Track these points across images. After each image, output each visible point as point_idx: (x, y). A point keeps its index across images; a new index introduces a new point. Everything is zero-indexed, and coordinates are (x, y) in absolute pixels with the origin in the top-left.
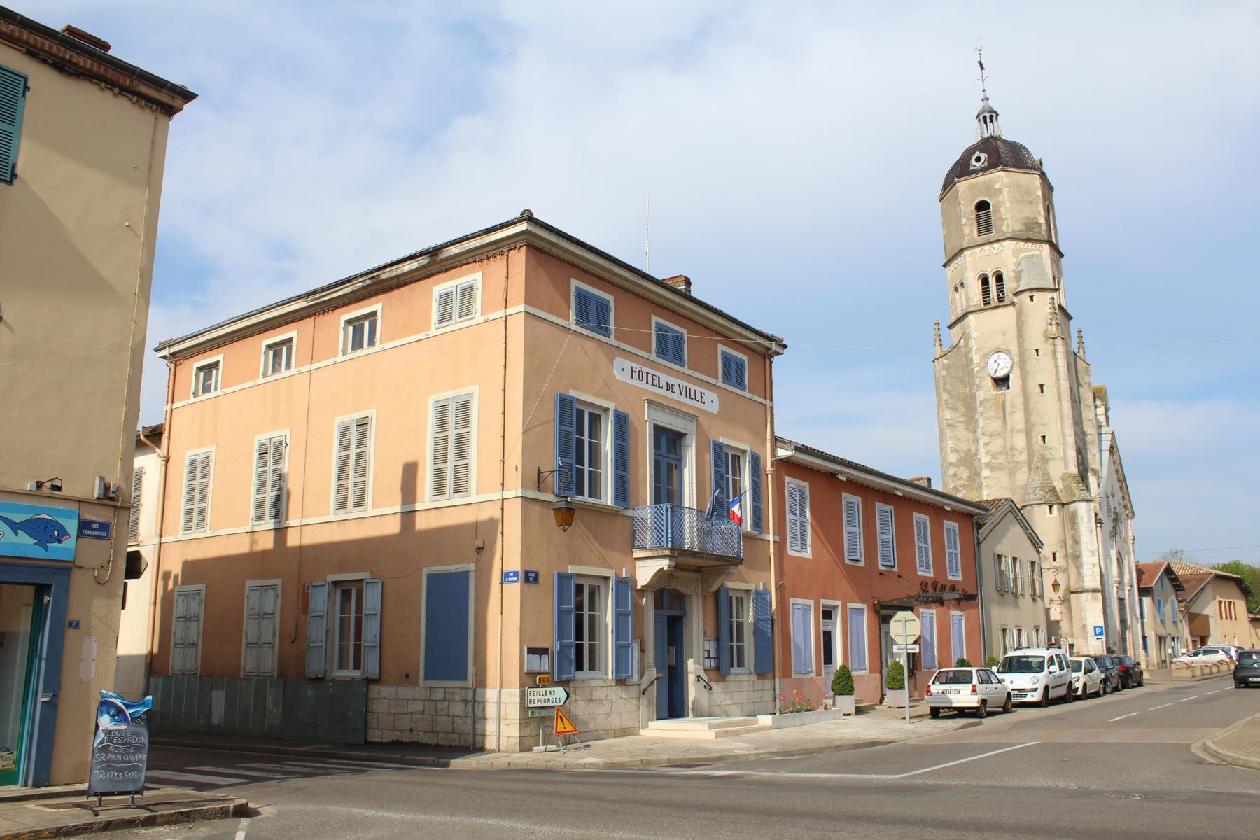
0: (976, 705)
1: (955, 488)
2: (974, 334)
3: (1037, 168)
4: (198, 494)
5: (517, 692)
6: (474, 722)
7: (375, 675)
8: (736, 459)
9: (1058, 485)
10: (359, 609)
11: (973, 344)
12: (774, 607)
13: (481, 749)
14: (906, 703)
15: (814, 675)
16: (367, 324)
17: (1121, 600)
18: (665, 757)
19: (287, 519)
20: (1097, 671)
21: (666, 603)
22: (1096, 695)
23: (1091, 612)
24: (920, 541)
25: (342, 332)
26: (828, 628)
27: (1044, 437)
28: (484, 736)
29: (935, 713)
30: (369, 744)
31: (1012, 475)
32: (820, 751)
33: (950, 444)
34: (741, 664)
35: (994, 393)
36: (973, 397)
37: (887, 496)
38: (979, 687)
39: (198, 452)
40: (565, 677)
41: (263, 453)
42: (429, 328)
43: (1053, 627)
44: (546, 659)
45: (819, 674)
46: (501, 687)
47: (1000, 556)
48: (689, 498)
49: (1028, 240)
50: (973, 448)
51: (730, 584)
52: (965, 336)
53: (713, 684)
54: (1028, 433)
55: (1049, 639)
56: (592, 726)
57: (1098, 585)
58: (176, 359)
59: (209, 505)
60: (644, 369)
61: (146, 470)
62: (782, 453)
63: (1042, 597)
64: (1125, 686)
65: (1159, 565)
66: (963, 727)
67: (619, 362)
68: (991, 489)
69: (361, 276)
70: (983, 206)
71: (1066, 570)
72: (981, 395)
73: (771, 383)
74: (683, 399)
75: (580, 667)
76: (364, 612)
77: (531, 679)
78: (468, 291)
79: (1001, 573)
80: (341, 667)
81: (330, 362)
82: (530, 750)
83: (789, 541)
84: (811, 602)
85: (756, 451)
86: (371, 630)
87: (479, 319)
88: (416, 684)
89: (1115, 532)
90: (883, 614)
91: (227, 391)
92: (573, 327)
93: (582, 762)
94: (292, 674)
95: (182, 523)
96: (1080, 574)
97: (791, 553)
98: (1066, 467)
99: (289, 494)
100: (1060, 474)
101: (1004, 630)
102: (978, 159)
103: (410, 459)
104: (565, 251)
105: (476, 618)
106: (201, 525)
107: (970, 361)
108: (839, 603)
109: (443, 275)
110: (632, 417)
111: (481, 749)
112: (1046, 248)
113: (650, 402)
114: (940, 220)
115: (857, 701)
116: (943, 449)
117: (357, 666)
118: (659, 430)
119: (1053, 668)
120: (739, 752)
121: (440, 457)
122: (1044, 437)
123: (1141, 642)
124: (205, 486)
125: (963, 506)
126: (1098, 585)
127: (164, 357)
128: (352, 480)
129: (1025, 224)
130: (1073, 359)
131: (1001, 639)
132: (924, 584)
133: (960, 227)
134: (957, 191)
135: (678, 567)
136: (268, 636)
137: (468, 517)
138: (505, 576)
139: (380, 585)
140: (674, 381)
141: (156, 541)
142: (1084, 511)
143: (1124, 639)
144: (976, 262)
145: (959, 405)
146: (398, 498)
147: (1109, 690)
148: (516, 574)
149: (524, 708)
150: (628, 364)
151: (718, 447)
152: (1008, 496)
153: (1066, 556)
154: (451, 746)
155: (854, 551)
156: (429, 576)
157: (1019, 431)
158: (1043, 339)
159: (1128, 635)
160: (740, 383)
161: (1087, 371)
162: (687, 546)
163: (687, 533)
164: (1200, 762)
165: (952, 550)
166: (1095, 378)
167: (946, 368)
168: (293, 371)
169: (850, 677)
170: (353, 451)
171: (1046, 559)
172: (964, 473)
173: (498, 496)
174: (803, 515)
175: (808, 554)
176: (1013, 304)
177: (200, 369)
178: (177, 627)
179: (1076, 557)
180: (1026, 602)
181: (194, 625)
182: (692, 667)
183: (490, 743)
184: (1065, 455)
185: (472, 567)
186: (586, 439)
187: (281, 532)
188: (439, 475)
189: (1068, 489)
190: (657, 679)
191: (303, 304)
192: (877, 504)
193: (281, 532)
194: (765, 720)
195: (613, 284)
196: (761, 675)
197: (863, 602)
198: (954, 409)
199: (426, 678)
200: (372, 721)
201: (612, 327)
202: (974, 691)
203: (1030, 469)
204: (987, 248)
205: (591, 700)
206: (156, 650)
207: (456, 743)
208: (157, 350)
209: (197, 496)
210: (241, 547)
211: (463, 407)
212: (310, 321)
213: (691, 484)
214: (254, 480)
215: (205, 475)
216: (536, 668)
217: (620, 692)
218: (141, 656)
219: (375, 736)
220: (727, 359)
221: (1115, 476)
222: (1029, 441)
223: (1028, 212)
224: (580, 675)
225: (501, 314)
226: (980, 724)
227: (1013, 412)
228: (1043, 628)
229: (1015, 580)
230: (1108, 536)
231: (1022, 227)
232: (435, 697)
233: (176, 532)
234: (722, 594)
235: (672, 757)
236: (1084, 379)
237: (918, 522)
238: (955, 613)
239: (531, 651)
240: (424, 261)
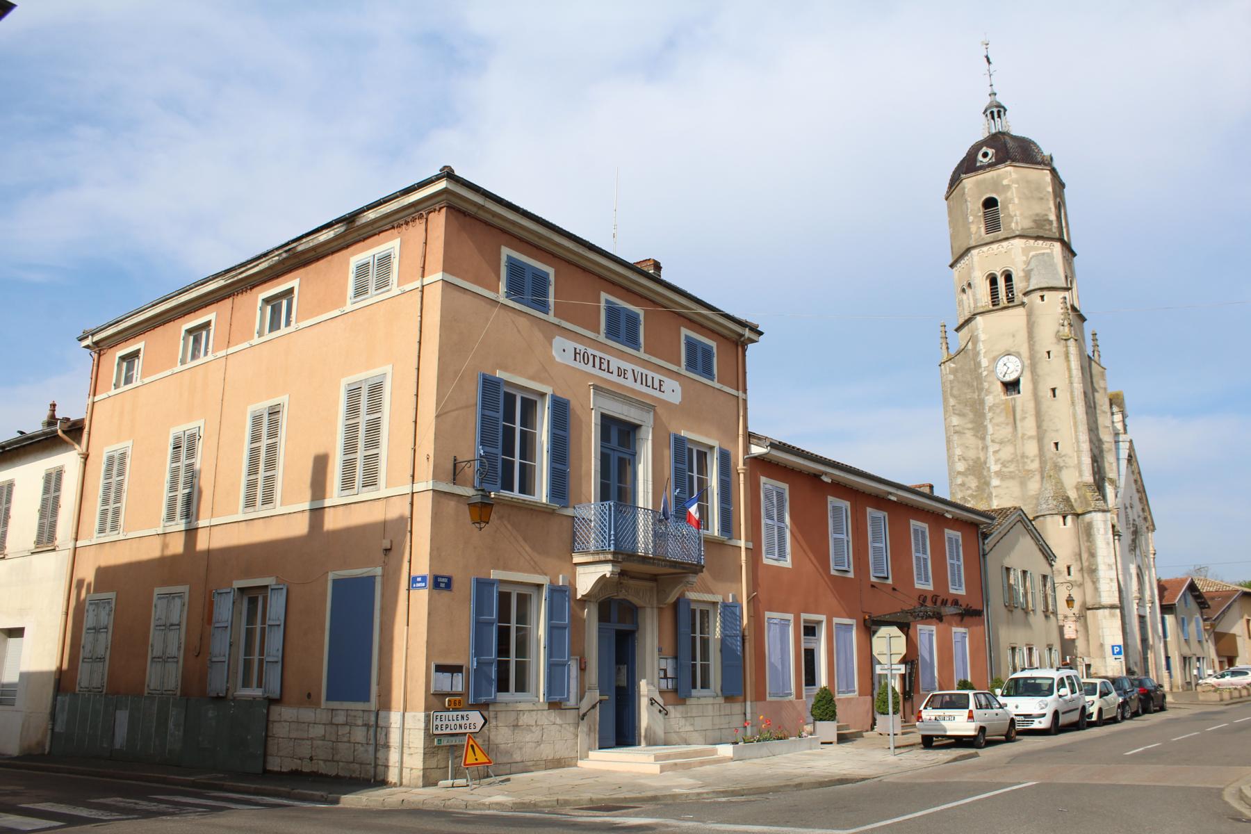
0: (973, 733)
1: (964, 498)
2: (982, 337)
3: (1047, 163)
4: (113, 493)
5: (422, 715)
6: (376, 751)
7: (276, 695)
8: (702, 456)
9: (1073, 495)
10: (263, 622)
11: (981, 347)
12: (745, 621)
13: (383, 783)
14: (899, 731)
15: (793, 697)
16: (285, 303)
17: (1142, 618)
18: (586, 796)
19: (197, 519)
20: (1114, 694)
21: (614, 615)
22: (1113, 720)
23: (1109, 630)
24: (917, 551)
25: (259, 312)
26: (810, 646)
27: (1056, 444)
28: (387, 767)
29: (928, 742)
30: (266, 774)
31: (1023, 484)
32: (776, 790)
33: (958, 452)
34: (705, 685)
35: (1004, 397)
36: (982, 402)
37: (880, 501)
38: (976, 713)
39: (114, 448)
40: (483, 699)
41: (177, 447)
42: (344, 303)
43: (1068, 646)
44: (459, 679)
45: (799, 696)
46: (405, 710)
47: (1008, 569)
48: (644, 495)
49: (1038, 238)
50: (982, 455)
51: (692, 595)
52: (973, 339)
53: (670, 708)
54: (1040, 439)
55: (1064, 659)
56: (517, 757)
57: (1116, 601)
58: (100, 348)
59: (123, 505)
60: (590, 351)
61: (66, 468)
62: (756, 450)
63: (1055, 613)
64: (1146, 711)
65: (1183, 581)
66: (955, 760)
67: (559, 342)
68: (1002, 497)
69: (277, 249)
70: (990, 203)
71: (1081, 585)
72: (989, 400)
73: (745, 373)
74: (638, 387)
75: (503, 686)
76: (268, 622)
77: (437, 701)
78: (385, 261)
79: (1010, 587)
80: (246, 684)
81: (246, 345)
82: (436, 784)
83: (764, 548)
84: (790, 617)
85: (726, 447)
86: (275, 641)
87: (395, 290)
88: (318, 704)
90: (870, 627)
91: (146, 380)
92: (502, 299)
93: (487, 800)
94: (195, 693)
95: (97, 526)
96: (1096, 589)
97: (767, 561)
98: (1081, 475)
99: (200, 492)
101: (1013, 649)
102: (985, 155)
103: (321, 451)
104: (495, 214)
105: (381, 630)
106: (114, 528)
107: (978, 365)
108: (823, 618)
109: (361, 244)
110: (574, 404)
111: (383, 783)
112: (1057, 245)
113: (596, 388)
114: (946, 218)
115: (839, 728)
116: (950, 456)
117: (260, 685)
118: (607, 422)
119: (1062, 691)
120: (677, 791)
121: (350, 447)
122: (1056, 444)
123: (1164, 662)
124: (120, 484)
125: (965, 514)
126: (1116, 601)
127: (87, 347)
128: (261, 474)
129: (1035, 221)
130: (1088, 363)
131: (1010, 658)
132: (923, 597)
133: (966, 224)
134: (964, 188)
135: (623, 573)
136: (173, 650)
137: (375, 515)
138: (412, 581)
139: (284, 591)
140: (625, 365)
141: (71, 545)
142: (1100, 523)
143: (1145, 659)
144: (984, 262)
145: (967, 410)
146: (308, 494)
147: (1128, 715)
148: (424, 579)
149: (429, 736)
150: (570, 345)
151: (680, 442)
152: (1017, 505)
154: (351, 778)
155: (841, 558)
156: (334, 581)
157: (1030, 438)
158: (1054, 340)
159: (1150, 655)
160: (708, 372)
161: (1103, 375)
162: (641, 552)
163: (641, 538)
164: (1238, 818)
165: (954, 562)
166: (1111, 383)
167: (954, 372)
168: (210, 357)
169: (831, 700)
170: (264, 442)
171: (1060, 572)
172: (973, 483)
173: (407, 489)
174: (781, 519)
175: (787, 563)
176: (1023, 304)
177: (123, 358)
178: (86, 639)
179: (1093, 571)
180: (1037, 619)
181: (102, 637)
182: (645, 688)
183: (393, 776)
184: (1080, 463)
185: (378, 571)
186: (518, 427)
187: (191, 533)
188: (349, 466)
189: (1083, 498)
190: (600, 701)
191: (220, 283)
192: (869, 510)
193: (191, 533)
194: (726, 750)
195: (554, 255)
196: (729, 698)
197: (850, 617)
199: (328, 699)
200: (272, 748)
201: (551, 300)
202: (971, 717)
203: (1042, 478)
204: (995, 246)
205: (516, 726)
206: (65, 666)
207: (356, 775)
208: (81, 340)
209: (112, 495)
210: (152, 551)
211: (376, 389)
212: (228, 302)
213: (646, 481)
214: (168, 477)
215: (121, 473)
216: (447, 688)
217: (554, 716)
218: (41, 674)
219: (274, 764)
220: (691, 344)
221: (1134, 486)
222: (1041, 448)
223: (1037, 208)
224: (502, 697)
225: (418, 284)
226: (976, 755)
227: (1024, 418)
228: (1057, 647)
229: (1025, 595)
230: (1127, 549)
232: (335, 721)
233: (91, 536)
234: (682, 608)
235: (594, 797)
236: (1099, 383)
237: (916, 531)
238: (958, 630)
239: (440, 668)
240: (339, 229)
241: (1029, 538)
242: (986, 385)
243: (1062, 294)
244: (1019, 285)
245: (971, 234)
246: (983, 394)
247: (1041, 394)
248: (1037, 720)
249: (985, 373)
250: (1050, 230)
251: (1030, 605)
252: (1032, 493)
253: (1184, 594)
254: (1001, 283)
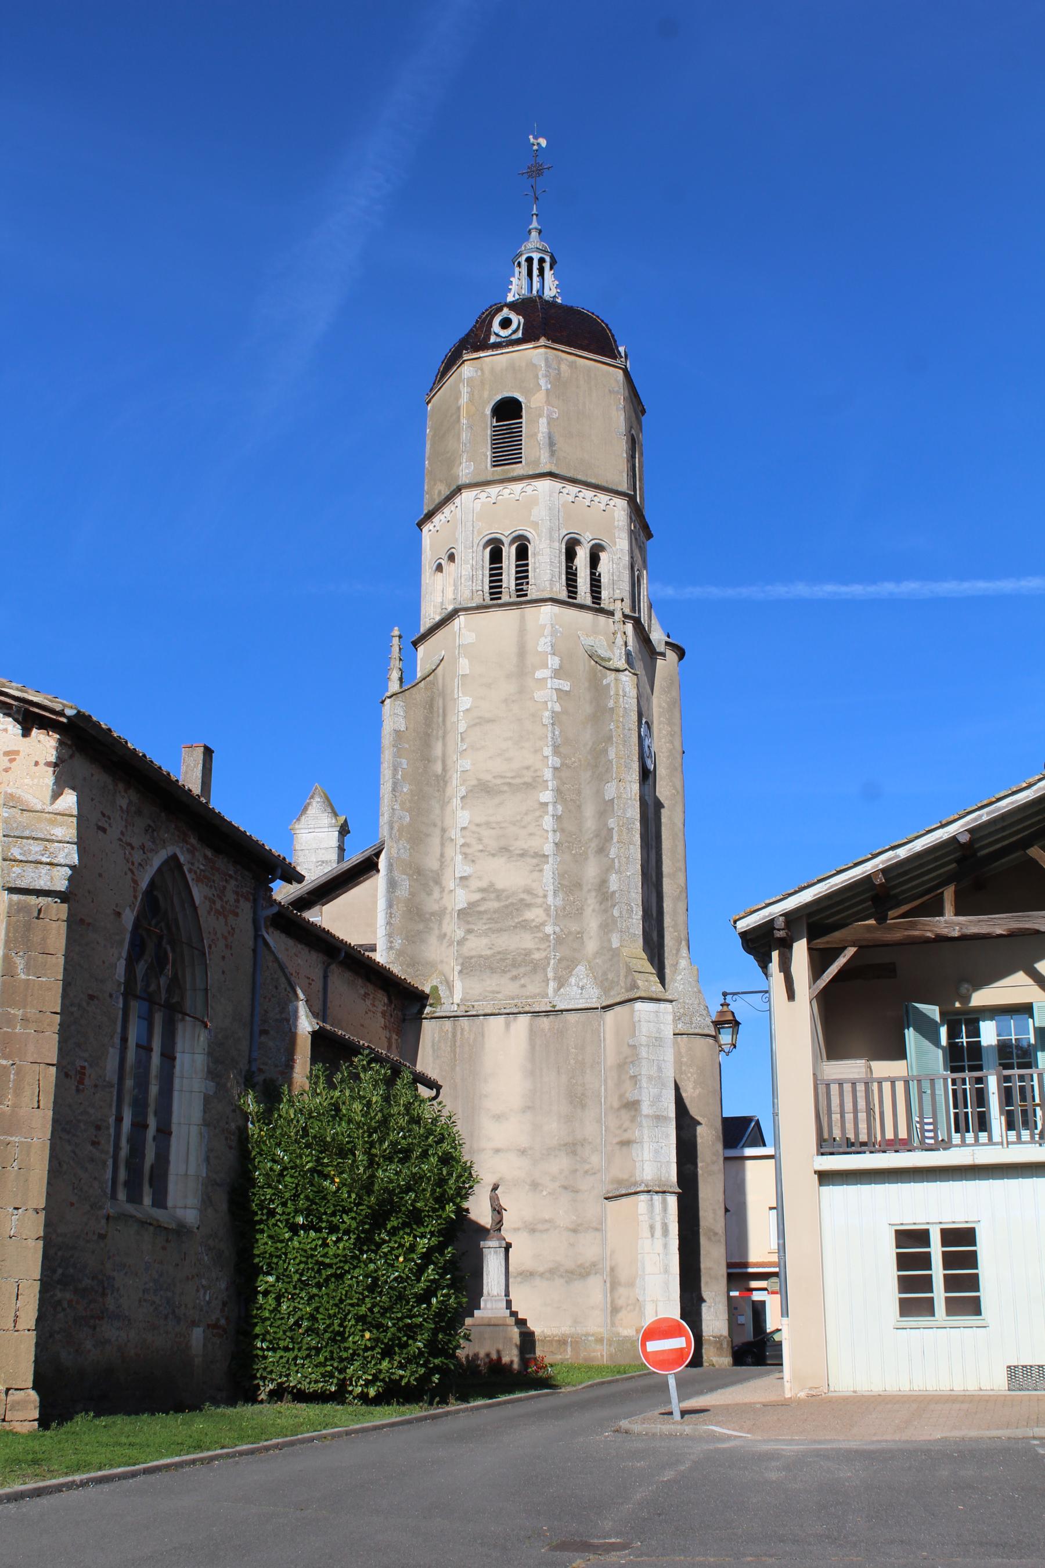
102: (506, 323)
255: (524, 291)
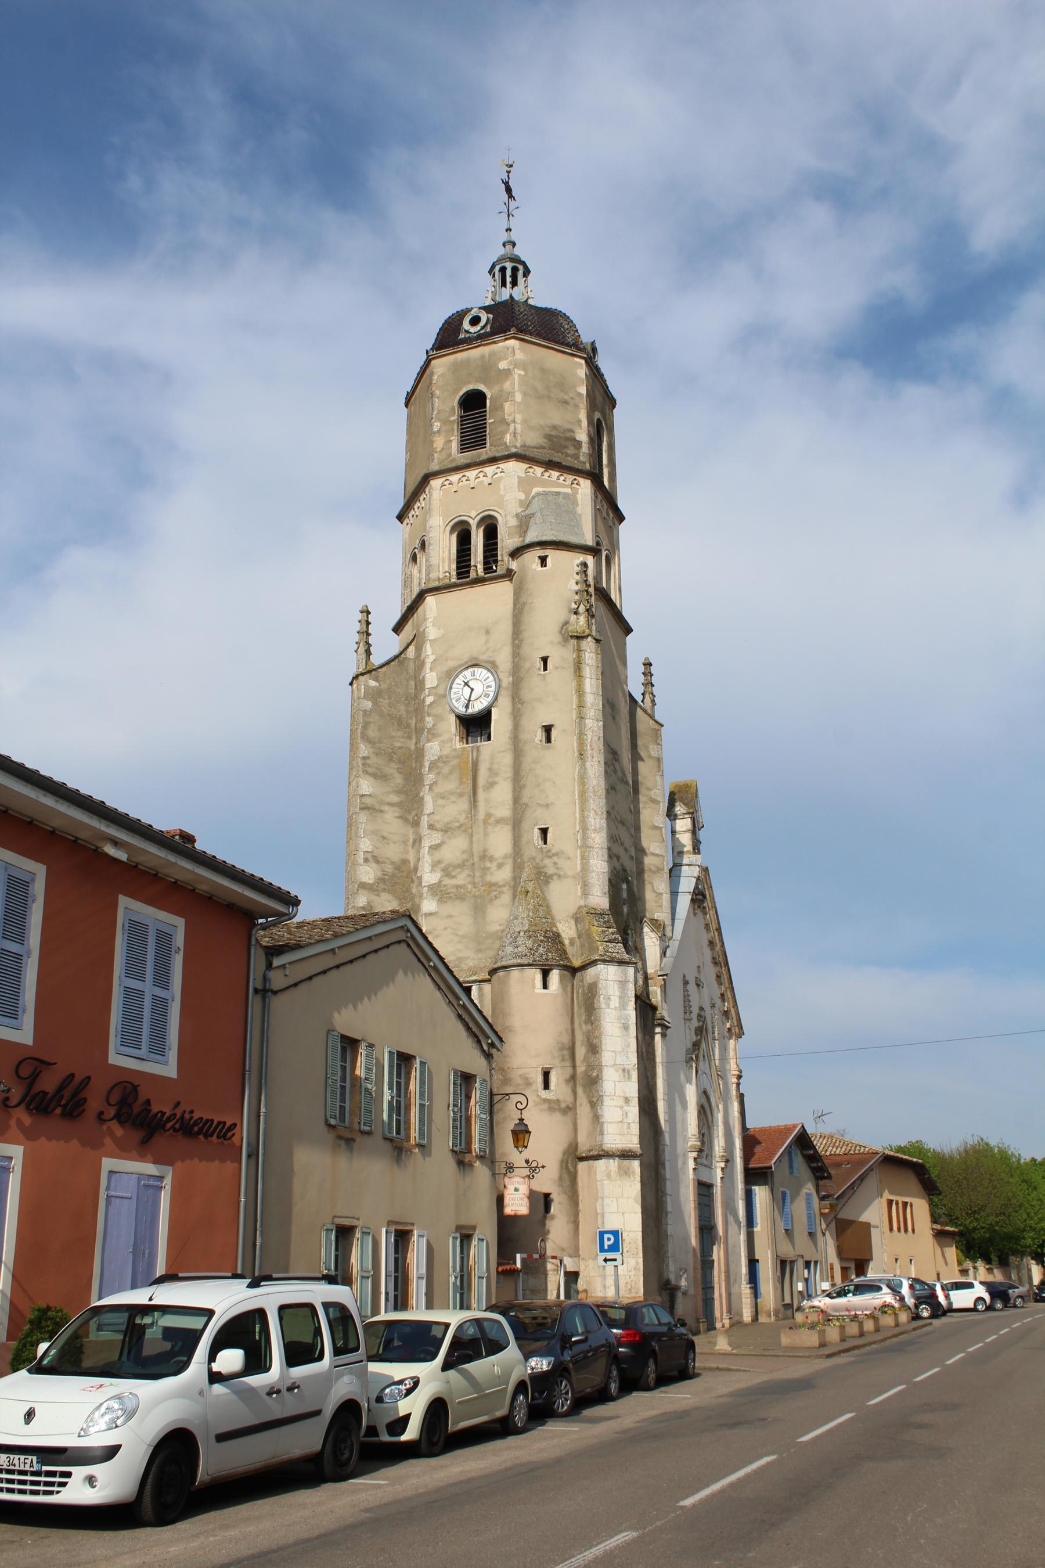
2: (432, 633)
9: (567, 931)
17: (704, 1188)
20: (512, 1352)
22: (501, 1429)
23: (617, 1200)
27: (544, 832)
31: (479, 910)
33: (365, 845)
35: (458, 745)
36: (420, 753)
47: (350, 1044)
49: (550, 465)
50: (411, 857)
54: (517, 823)
57: (632, 1140)
63: (489, 1158)
64: (630, 1384)
65: (788, 1130)
71: (569, 1110)
72: (433, 749)
89: (696, 1051)
96: (596, 1118)
98: (585, 893)
100: (573, 909)
101: (344, 1234)
112: (585, 487)
122: (544, 832)
123: (744, 1270)
129: (549, 437)
142: (613, 984)
143: (706, 1264)
145: (391, 769)
147: (563, 1404)
153: (573, 1078)
157: (499, 821)
158: (558, 638)
159: (718, 1254)
161: (656, 736)
167: (374, 695)
176: (509, 574)
179: (589, 1082)
184: (585, 868)
189: (585, 936)
198: (379, 776)
203: (514, 896)
204: (472, 474)
221: (708, 953)
223: (556, 417)
227: (492, 785)
229: (400, 1108)
230: (682, 1056)
231: (542, 441)
241: (424, 984)
242: (429, 721)
243: (580, 558)
244: (507, 541)
245: (434, 451)
246: (423, 738)
247: (524, 736)
248: (79, 1472)
249: (429, 700)
250: (576, 457)
251: (414, 1133)
252: (495, 927)
253: (790, 1146)
254: (478, 540)
255: (498, 299)
